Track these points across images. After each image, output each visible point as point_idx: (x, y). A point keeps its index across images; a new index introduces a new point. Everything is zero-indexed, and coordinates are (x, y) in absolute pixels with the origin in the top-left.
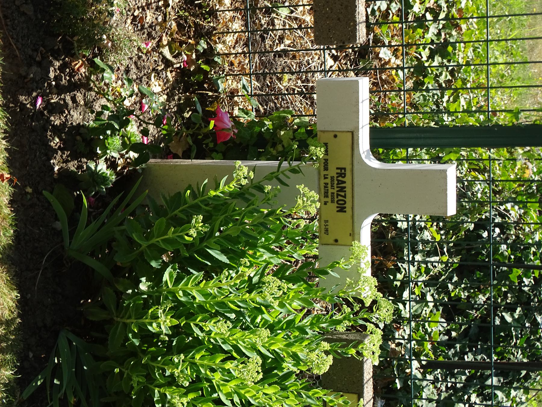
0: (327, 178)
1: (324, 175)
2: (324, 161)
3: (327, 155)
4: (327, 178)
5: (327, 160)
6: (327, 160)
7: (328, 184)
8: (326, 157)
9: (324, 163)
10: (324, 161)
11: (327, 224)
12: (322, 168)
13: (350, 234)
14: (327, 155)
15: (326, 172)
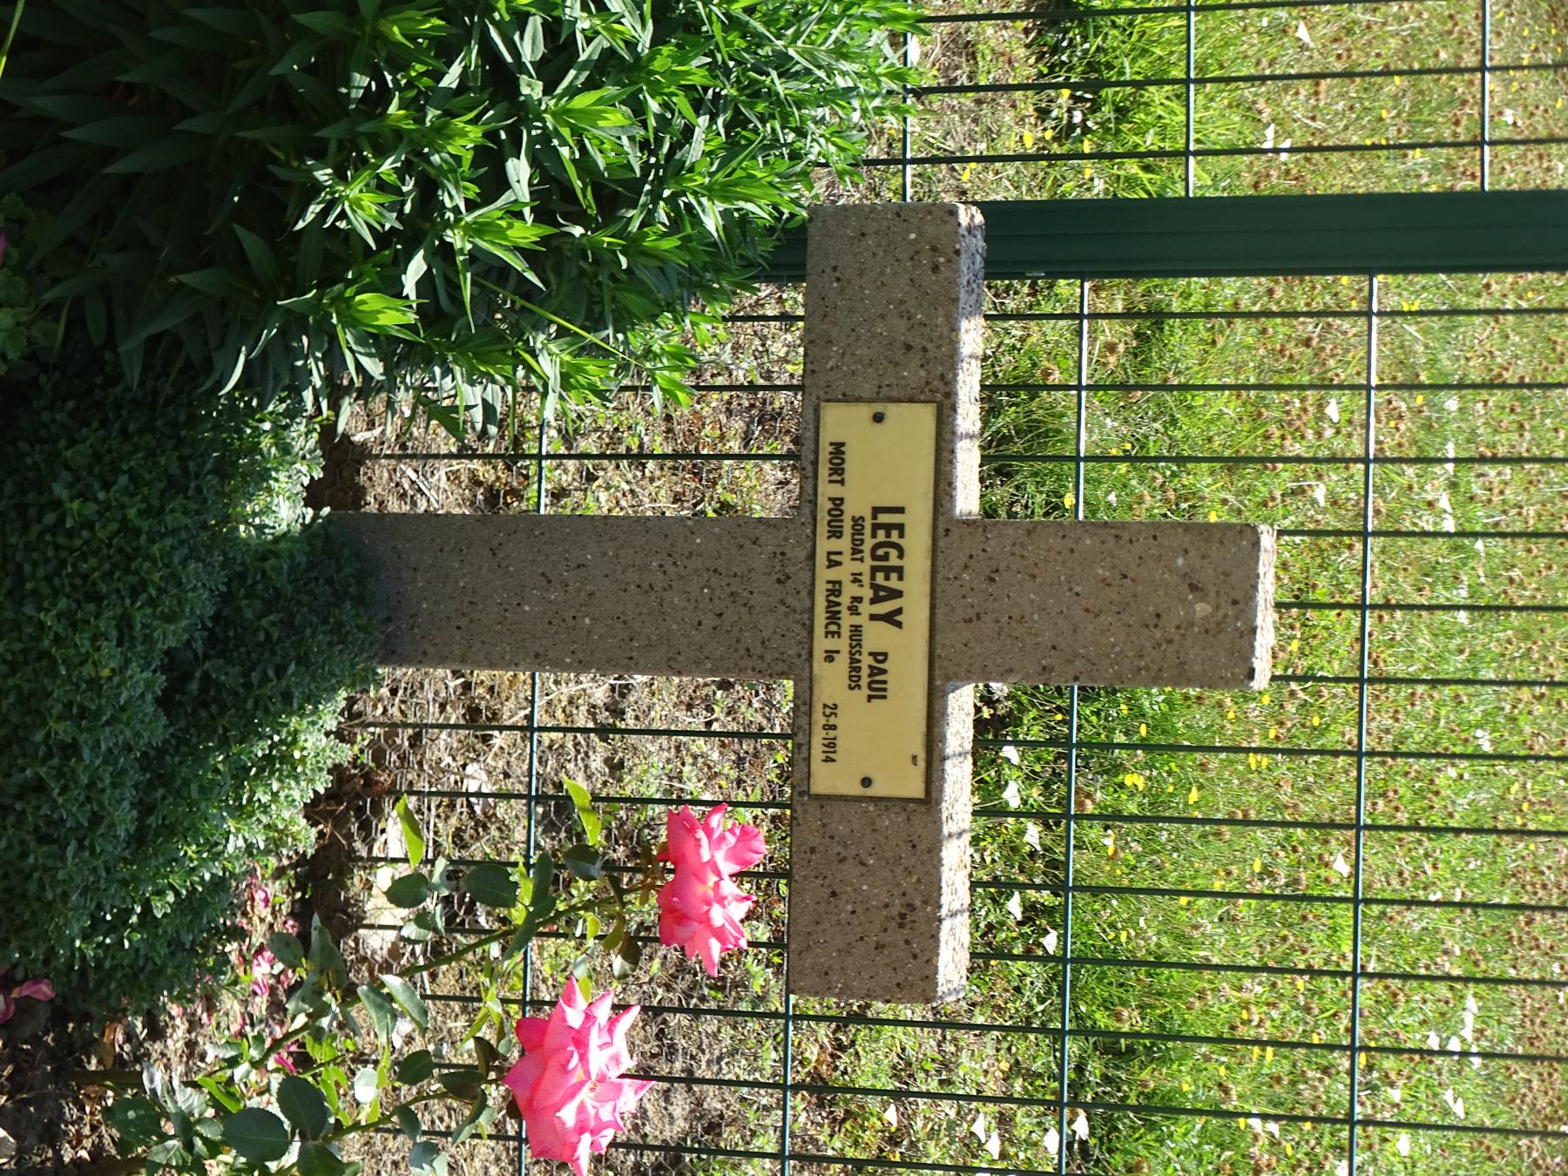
0: (839, 564)
1: (829, 553)
2: (830, 505)
3: (842, 482)
4: (839, 564)
5: (842, 500)
6: (842, 500)
7: (840, 583)
8: (836, 491)
9: (829, 512)
10: (830, 505)
11: (832, 720)
12: (822, 529)
13: (914, 758)
14: (842, 482)
15: (835, 545)
